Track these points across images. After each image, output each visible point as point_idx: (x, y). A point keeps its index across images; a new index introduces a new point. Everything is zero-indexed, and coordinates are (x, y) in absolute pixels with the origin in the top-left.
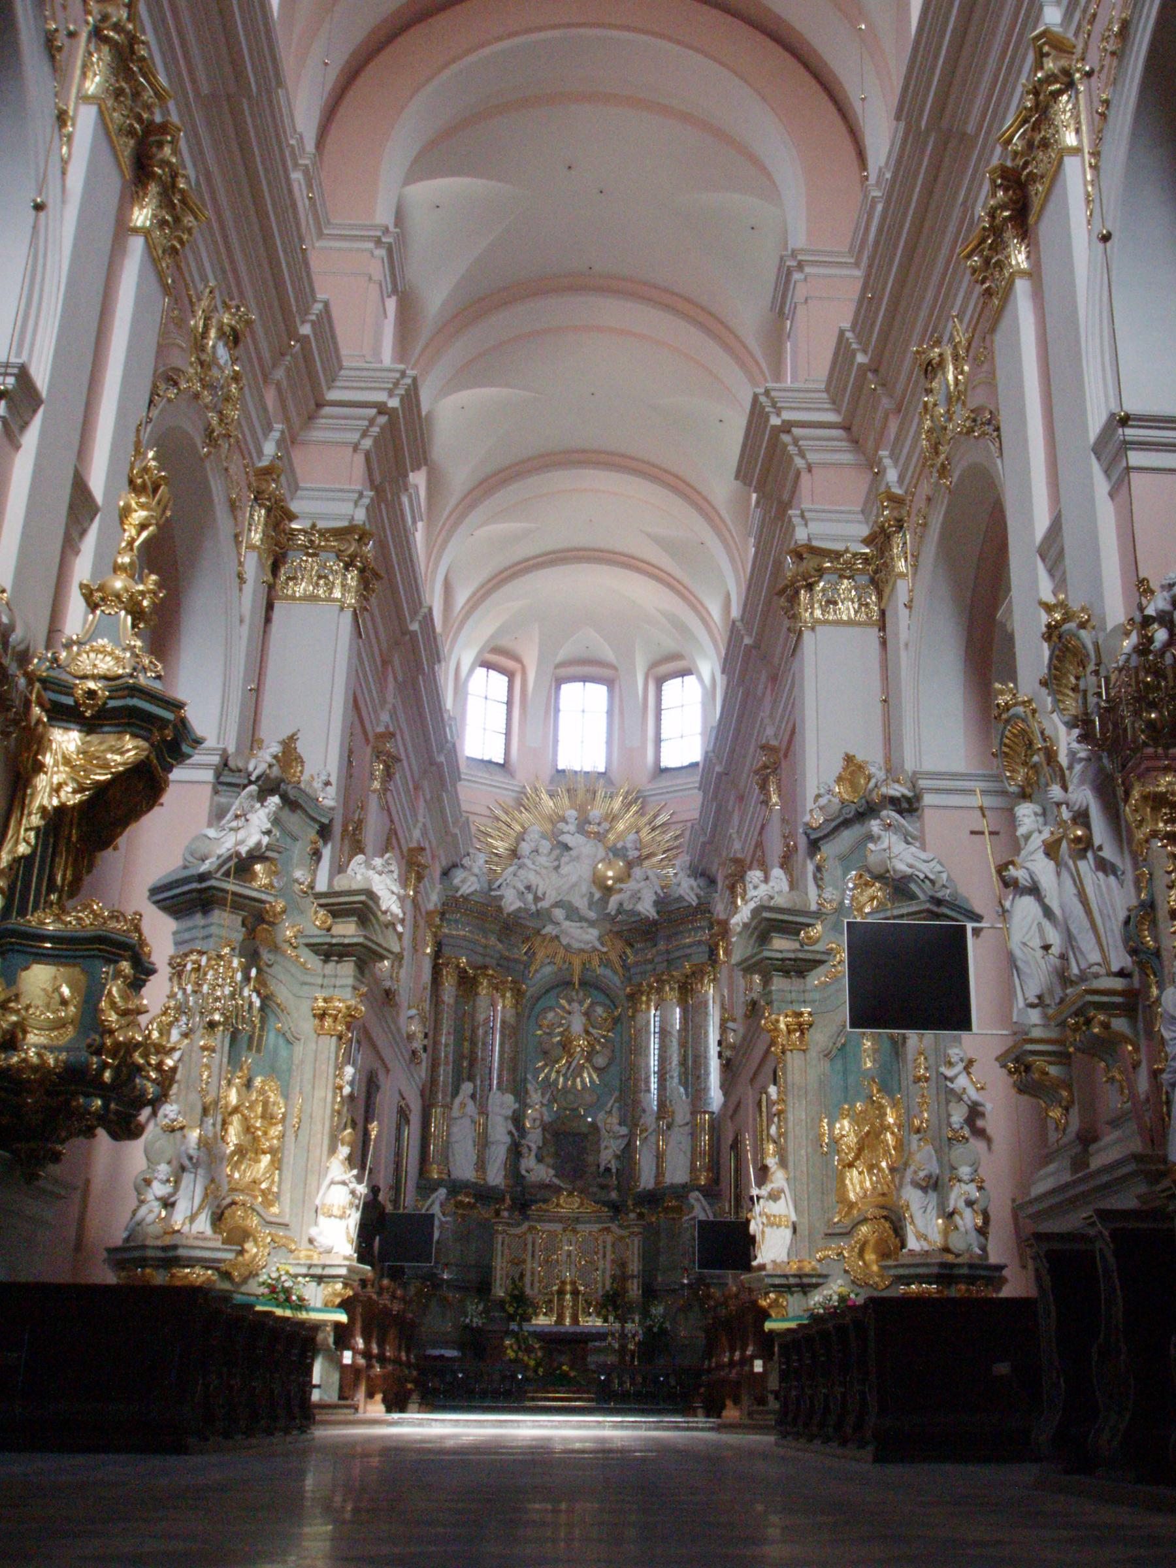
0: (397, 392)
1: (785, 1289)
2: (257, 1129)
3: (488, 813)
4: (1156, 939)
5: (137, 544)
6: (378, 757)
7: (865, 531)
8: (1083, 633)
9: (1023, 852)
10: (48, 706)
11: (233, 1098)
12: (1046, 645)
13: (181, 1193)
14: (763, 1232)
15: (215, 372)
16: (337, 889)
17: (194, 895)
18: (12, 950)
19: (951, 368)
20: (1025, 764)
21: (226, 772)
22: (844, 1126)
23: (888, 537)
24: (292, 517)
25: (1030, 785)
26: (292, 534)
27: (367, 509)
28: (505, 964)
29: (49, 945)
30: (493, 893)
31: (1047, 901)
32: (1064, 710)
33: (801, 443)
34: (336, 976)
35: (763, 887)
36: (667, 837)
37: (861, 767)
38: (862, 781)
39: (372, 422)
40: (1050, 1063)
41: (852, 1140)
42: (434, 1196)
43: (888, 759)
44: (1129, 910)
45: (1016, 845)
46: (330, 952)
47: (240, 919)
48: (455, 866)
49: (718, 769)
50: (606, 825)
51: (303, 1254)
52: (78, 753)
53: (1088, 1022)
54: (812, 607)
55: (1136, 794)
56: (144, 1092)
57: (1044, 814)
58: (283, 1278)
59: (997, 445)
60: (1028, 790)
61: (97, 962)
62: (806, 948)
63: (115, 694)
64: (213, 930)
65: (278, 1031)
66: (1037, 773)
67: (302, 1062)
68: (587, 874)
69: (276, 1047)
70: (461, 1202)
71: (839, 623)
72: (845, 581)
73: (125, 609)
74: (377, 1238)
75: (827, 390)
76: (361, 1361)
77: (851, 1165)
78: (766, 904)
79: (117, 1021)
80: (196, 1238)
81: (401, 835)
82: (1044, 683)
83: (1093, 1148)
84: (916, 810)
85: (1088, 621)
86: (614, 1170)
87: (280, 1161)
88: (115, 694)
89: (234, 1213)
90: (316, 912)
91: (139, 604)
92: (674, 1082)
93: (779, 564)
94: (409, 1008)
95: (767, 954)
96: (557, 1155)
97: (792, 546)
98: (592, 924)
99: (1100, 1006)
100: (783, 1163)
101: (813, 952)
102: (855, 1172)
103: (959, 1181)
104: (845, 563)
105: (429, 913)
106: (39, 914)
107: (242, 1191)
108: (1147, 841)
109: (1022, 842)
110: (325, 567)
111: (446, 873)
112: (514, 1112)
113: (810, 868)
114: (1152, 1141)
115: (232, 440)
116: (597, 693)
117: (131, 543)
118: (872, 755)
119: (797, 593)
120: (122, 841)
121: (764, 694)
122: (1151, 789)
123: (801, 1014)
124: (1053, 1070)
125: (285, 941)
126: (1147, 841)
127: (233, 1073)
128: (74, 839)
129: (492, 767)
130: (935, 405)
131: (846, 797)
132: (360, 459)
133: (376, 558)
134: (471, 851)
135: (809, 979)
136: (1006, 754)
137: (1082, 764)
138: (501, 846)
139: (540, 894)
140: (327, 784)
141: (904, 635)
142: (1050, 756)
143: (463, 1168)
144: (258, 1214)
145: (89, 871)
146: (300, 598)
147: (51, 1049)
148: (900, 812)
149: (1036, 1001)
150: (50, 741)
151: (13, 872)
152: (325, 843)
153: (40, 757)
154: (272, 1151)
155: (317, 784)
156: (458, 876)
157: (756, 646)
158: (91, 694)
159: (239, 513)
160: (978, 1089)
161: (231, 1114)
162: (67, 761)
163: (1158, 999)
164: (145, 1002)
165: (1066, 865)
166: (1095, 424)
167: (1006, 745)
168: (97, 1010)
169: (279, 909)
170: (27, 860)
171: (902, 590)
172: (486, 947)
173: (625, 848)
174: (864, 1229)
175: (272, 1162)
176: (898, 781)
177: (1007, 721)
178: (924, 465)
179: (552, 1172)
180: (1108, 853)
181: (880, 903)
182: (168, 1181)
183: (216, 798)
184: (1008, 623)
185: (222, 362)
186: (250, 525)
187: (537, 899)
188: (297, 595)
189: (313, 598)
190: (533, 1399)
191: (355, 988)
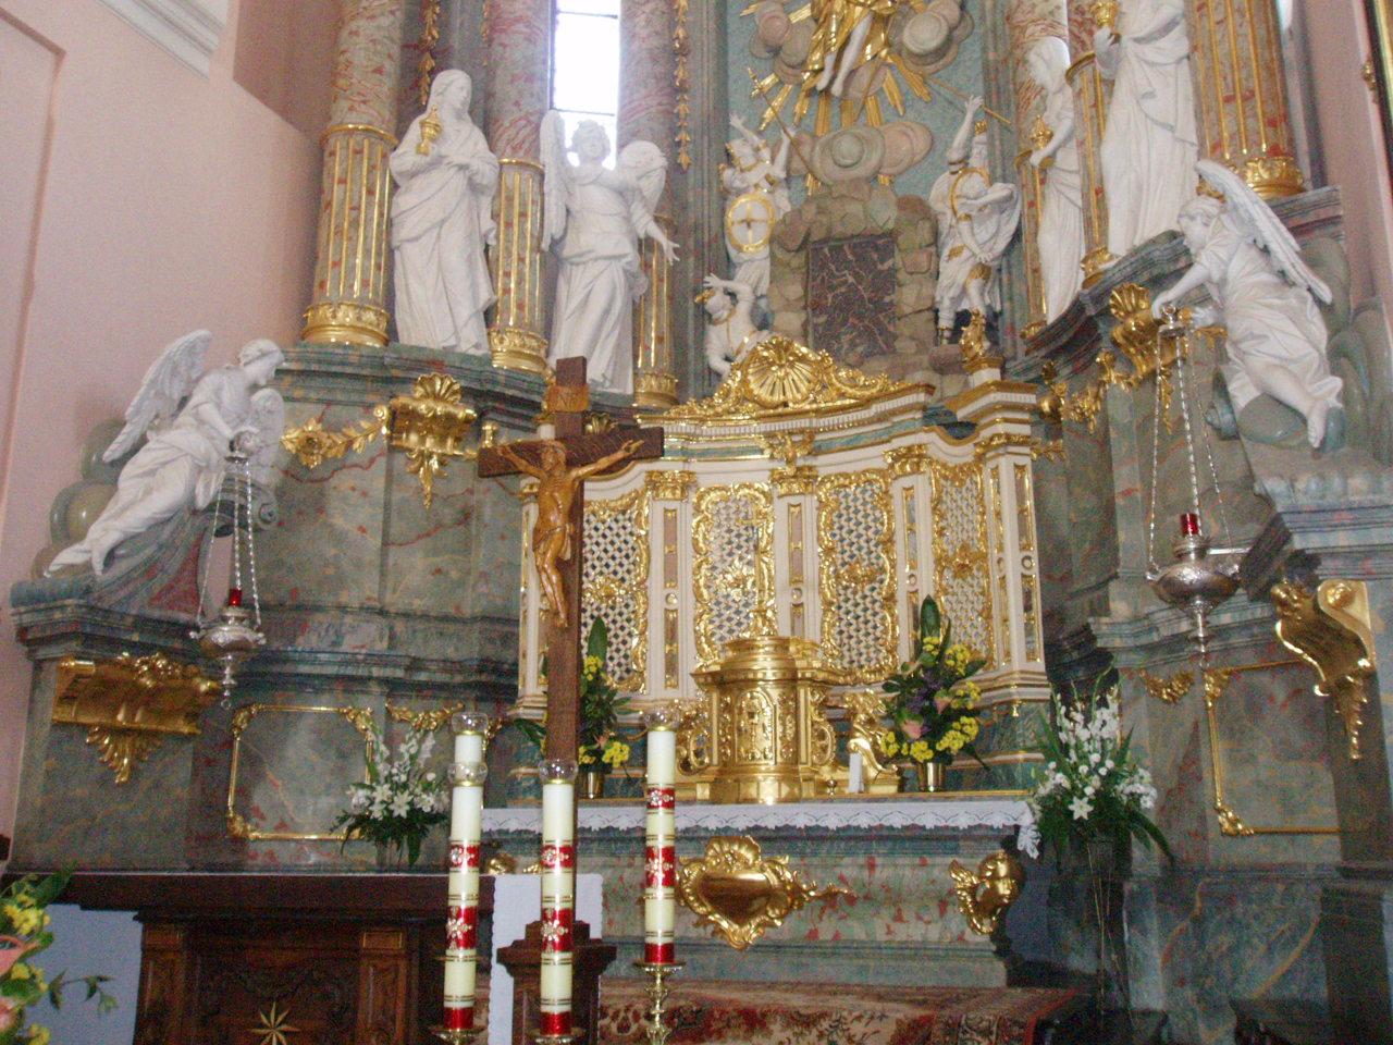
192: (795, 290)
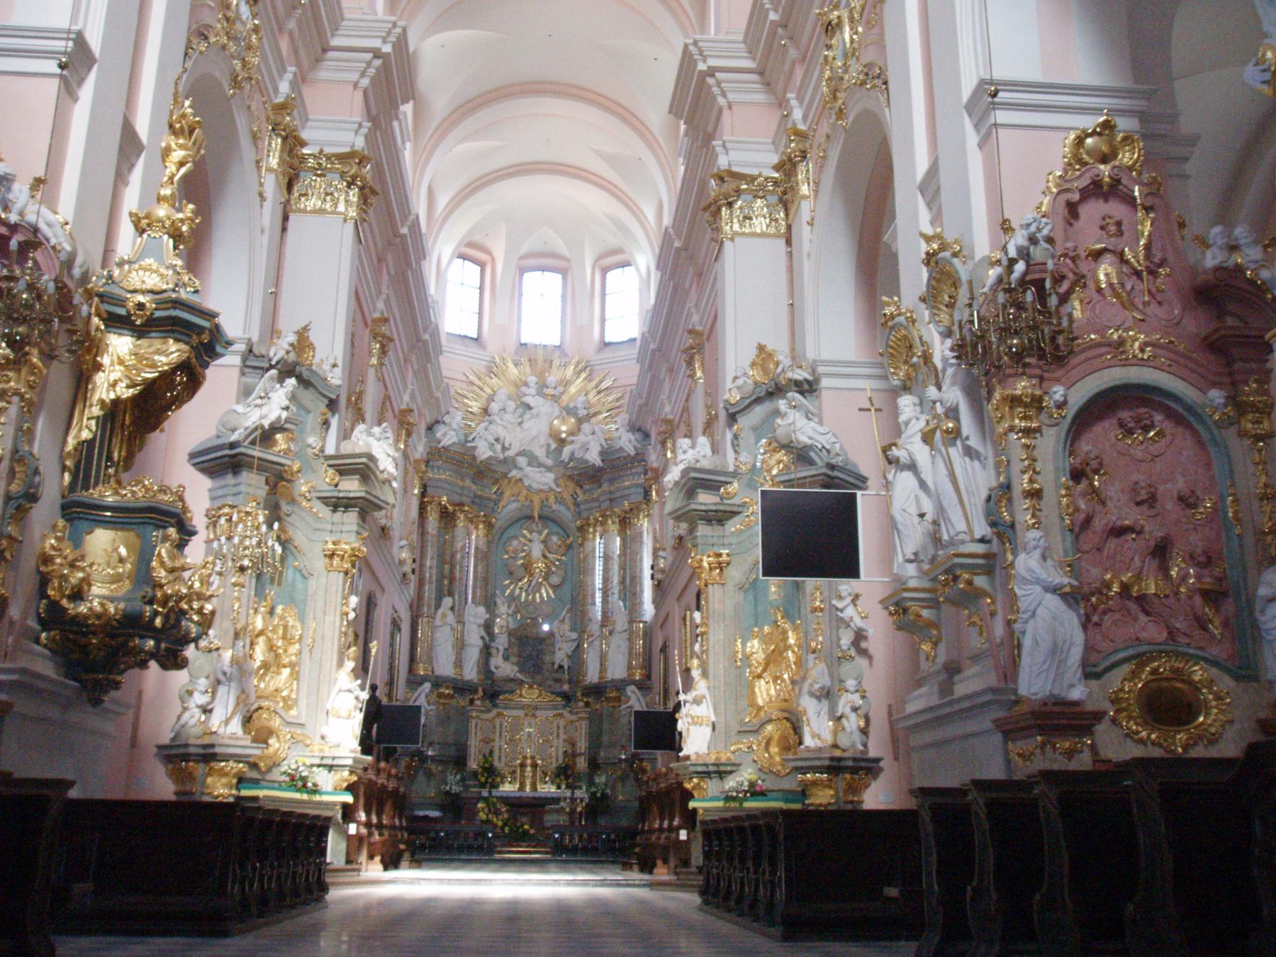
0: (389, 39)
1: (706, 775)
2: (279, 647)
3: (463, 378)
4: (1011, 515)
5: (176, 178)
6: (375, 338)
7: (775, 159)
8: (955, 261)
9: (903, 436)
10: (105, 316)
11: (259, 623)
12: (924, 269)
13: (217, 701)
14: (688, 729)
15: (238, 26)
16: (343, 452)
17: (226, 459)
18: (80, 518)
19: (847, 29)
20: (906, 362)
21: (251, 358)
22: (755, 646)
23: (794, 165)
24: (303, 144)
25: (910, 379)
26: (303, 159)
27: (366, 136)
28: (478, 501)
29: (109, 514)
30: (469, 445)
31: (922, 476)
32: (940, 322)
33: (723, 85)
34: (343, 523)
35: (691, 452)
36: (611, 399)
37: (770, 355)
38: (772, 366)
39: (369, 64)
40: (923, 607)
41: (760, 656)
42: (421, 689)
43: (793, 350)
44: (990, 490)
45: (897, 430)
46: (338, 504)
47: (264, 479)
48: (437, 422)
49: (652, 346)
50: (560, 389)
51: (316, 748)
52: (131, 355)
53: (956, 578)
54: (732, 222)
55: (997, 395)
56: (188, 632)
57: (921, 404)
58: (301, 769)
59: (886, 96)
60: (908, 383)
61: (150, 528)
62: (726, 501)
63: (160, 306)
64: (243, 488)
65: (295, 568)
66: (915, 370)
67: (315, 593)
68: (545, 429)
69: (293, 584)
70: (443, 693)
71: (754, 235)
72: (759, 200)
73: (168, 233)
74: (375, 726)
75: (744, 42)
76: (364, 831)
77: (759, 677)
78: (693, 466)
79: (166, 577)
80: (230, 738)
81: (393, 399)
82: (923, 300)
83: (957, 678)
84: (815, 390)
85: (960, 251)
86: (566, 667)
87: (298, 673)
88: (160, 306)
89: (260, 716)
90: (326, 471)
91: (179, 229)
92: (615, 598)
93: (703, 186)
94: (401, 539)
95: (693, 506)
96: (520, 656)
97: (715, 171)
98: (549, 469)
99: (962, 566)
100: (705, 674)
101: (730, 505)
102: (762, 682)
103: (846, 691)
104: (759, 185)
105: (416, 461)
106: (100, 487)
107: (267, 698)
108: (1005, 434)
109: (903, 428)
110: (331, 185)
111: (430, 428)
112: (486, 620)
113: (729, 436)
114: (1005, 676)
115: (253, 82)
116: (553, 281)
117: (171, 178)
118: (779, 345)
119: (719, 209)
120: (166, 424)
121: (691, 287)
122: (1009, 392)
123: (720, 555)
124: (925, 613)
125: (301, 495)
126: (1005, 434)
127: (259, 603)
128: (127, 422)
129: (467, 341)
130: (834, 59)
131: (758, 378)
132: (359, 96)
133: (373, 177)
134: (451, 409)
135: (726, 526)
136: (892, 355)
137: (953, 369)
138: (475, 406)
139: (507, 445)
140: (335, 366)
141: (806, 246)
142: (927, 358)
143: (445, 668)
144: (281, 716)
145: (140, 450)
146: (311, 212)
147: (112, 600)
148: (802, 393)
149: (913, 558)
150: (107, 344)
151: (78, 453)
152: (333, 414)
153: (98, 359)
154: (292, 665)
155: (326, 367)
156: (440, 431)
157: (685, 248)
158: (141, 306)
159: (260, 142)
160: (862, 618)
161: (258, 636)
162: (121, 362)
163: (1012, 565)
164: (189, 560)
165: (940, 451)
166: (967, 88)
167: (891, 347)
168: (149, 569)
169: (295, 469)
170: (90, 443)
171: (805, 208)
172: (463, 487)
173: (576, 408)
174: (769, 728)
175: (291, 674)
176: (801, 367)
177: (892, 328)
178: (824, 107)
179: (516, 669)
180: (974, 442)
181: (785, 466)
182: (206, 692)
183: (244, 379)
184: (893, 246)
185: (244, 17)
186: (269, 151)
187: (504, 449)
188: (308, 209)
189: (321, 211)
190: (500, 852)
191: (358, 533)
192: (515, 650)
